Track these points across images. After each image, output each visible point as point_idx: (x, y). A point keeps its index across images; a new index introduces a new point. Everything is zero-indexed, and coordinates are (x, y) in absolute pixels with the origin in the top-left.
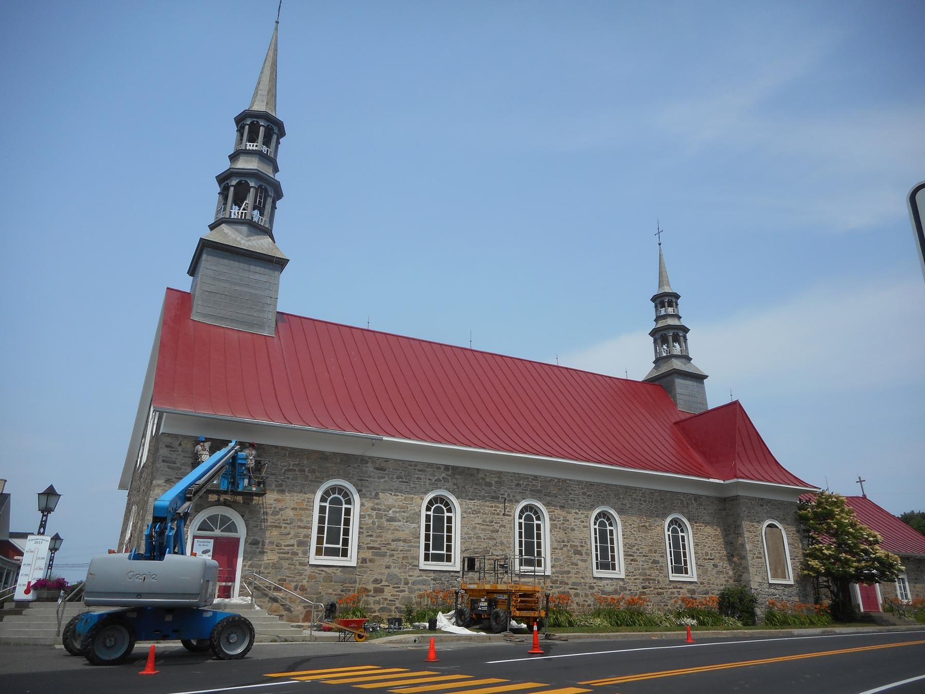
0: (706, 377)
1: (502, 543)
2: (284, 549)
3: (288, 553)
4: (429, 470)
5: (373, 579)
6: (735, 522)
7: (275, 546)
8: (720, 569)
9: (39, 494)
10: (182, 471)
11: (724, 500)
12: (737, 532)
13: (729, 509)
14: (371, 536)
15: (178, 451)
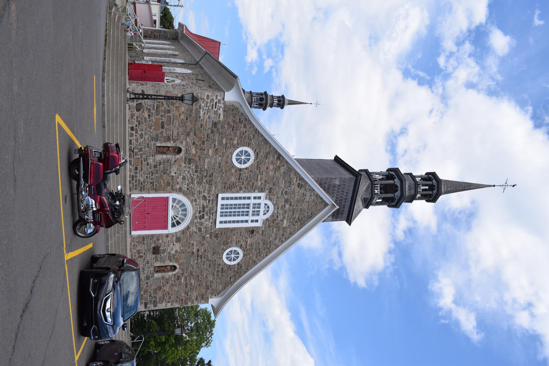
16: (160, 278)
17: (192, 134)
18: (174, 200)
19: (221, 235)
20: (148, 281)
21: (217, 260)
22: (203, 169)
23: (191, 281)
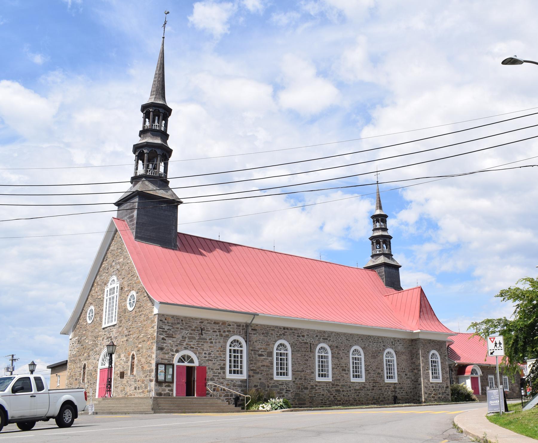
0: (400, 266)
1: (310, 366)
2: (215, 371)
3: (217, 373)
4: (276, 329)
5: (254, 385)
6: (417, 352)
7: (211, 370)
8: (408, 376)
9: (107, 345)
10: (168, 333)
11: (412, 340)
12: (417, 357)
13: (414, 345)
14: (252, 364)
15: (165, 323)
16: (137, 368)
17: (80, 358)
18: (102, 364)
19: (121, 317)
20: (137, 380)
21: (133, 315)
22: (92, 344)
23: (142, 336)
